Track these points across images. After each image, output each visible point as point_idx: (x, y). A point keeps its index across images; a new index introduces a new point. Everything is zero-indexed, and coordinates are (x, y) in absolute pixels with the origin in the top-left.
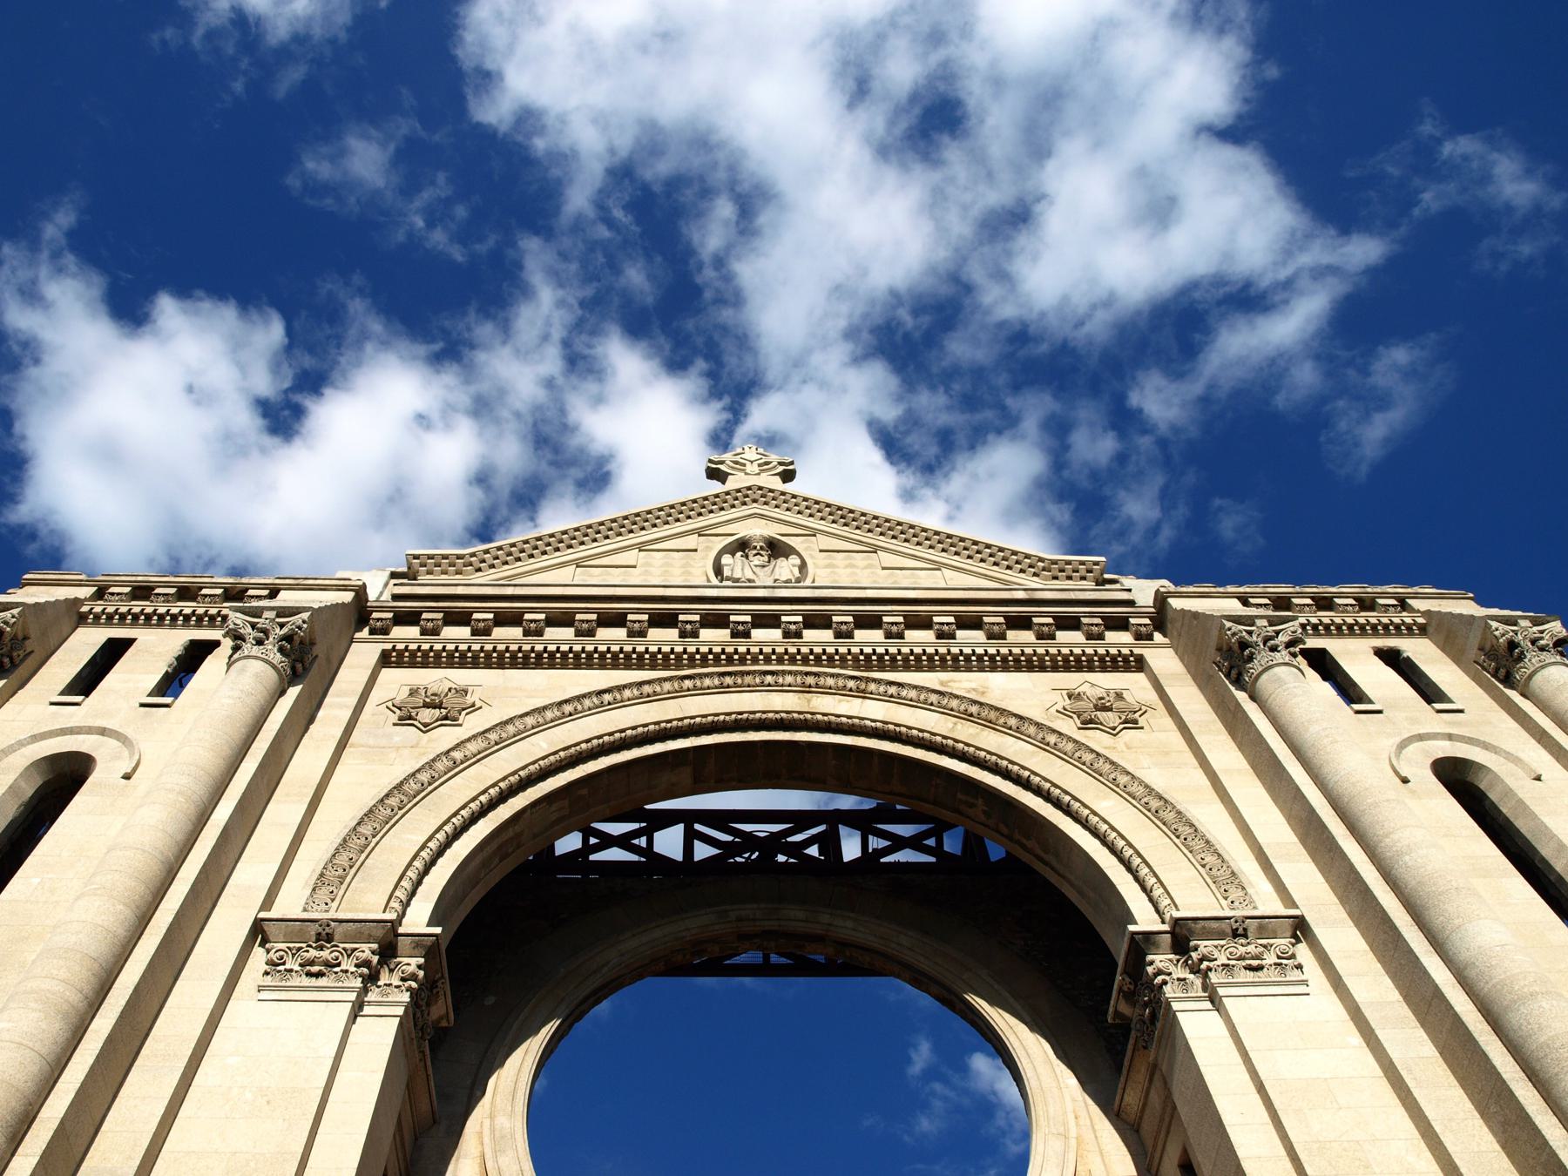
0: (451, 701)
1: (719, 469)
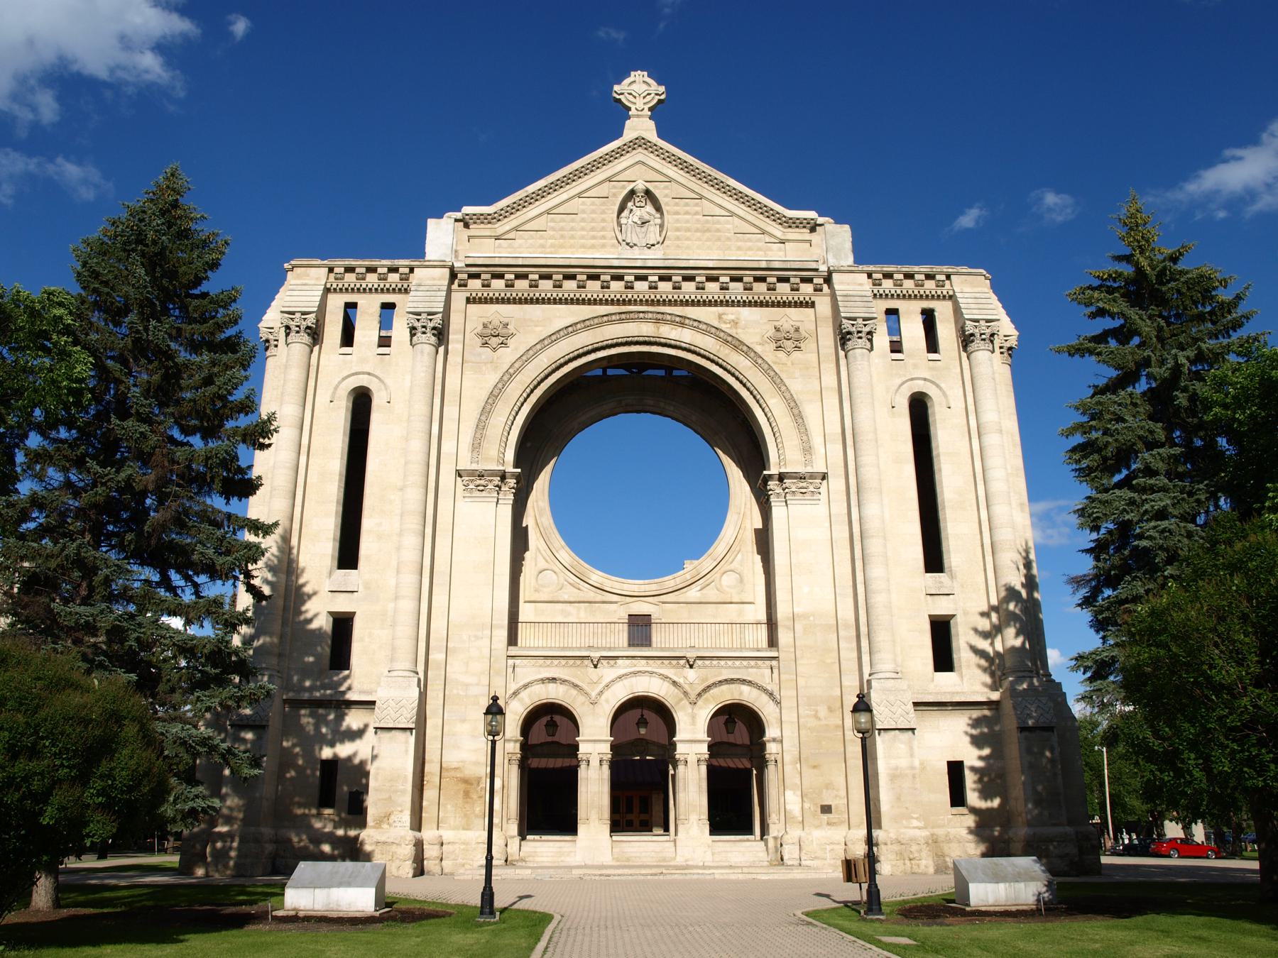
0: (502, 331)
1: (620, 99)
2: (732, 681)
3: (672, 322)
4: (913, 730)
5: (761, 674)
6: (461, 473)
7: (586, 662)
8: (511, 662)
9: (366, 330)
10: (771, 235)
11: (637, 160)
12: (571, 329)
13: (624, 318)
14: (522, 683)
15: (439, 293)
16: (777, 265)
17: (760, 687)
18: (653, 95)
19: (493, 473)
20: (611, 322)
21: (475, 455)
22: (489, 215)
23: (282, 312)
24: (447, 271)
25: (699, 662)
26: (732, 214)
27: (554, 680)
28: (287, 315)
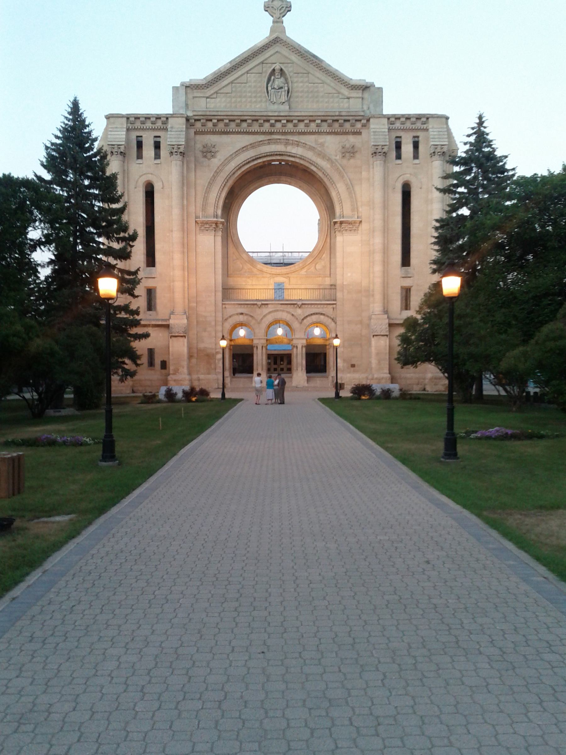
2: (317, 314)
3: (292, 144)
4: (387, 335)
5: (328, 310)
6: (199, 222)
7: (255, 306)
8: (224, 306)
9: (148, 151)
10: (343, 94)
11: (276, 50)
12: (244, 149)
13: (269, 142)
14: (228, 315)
15: (182, 133)
16: (343, 114)
17: (328, 316)
18: (284, 8)
19: (212, 222)
20: (264, 144)
21: (204, 213)
22: (203, 85)
23: (108, 145)
24: (184, 120)
25: (303, 306)
26: (323, 83)
27: (242, 314)
28: (110, 146)
